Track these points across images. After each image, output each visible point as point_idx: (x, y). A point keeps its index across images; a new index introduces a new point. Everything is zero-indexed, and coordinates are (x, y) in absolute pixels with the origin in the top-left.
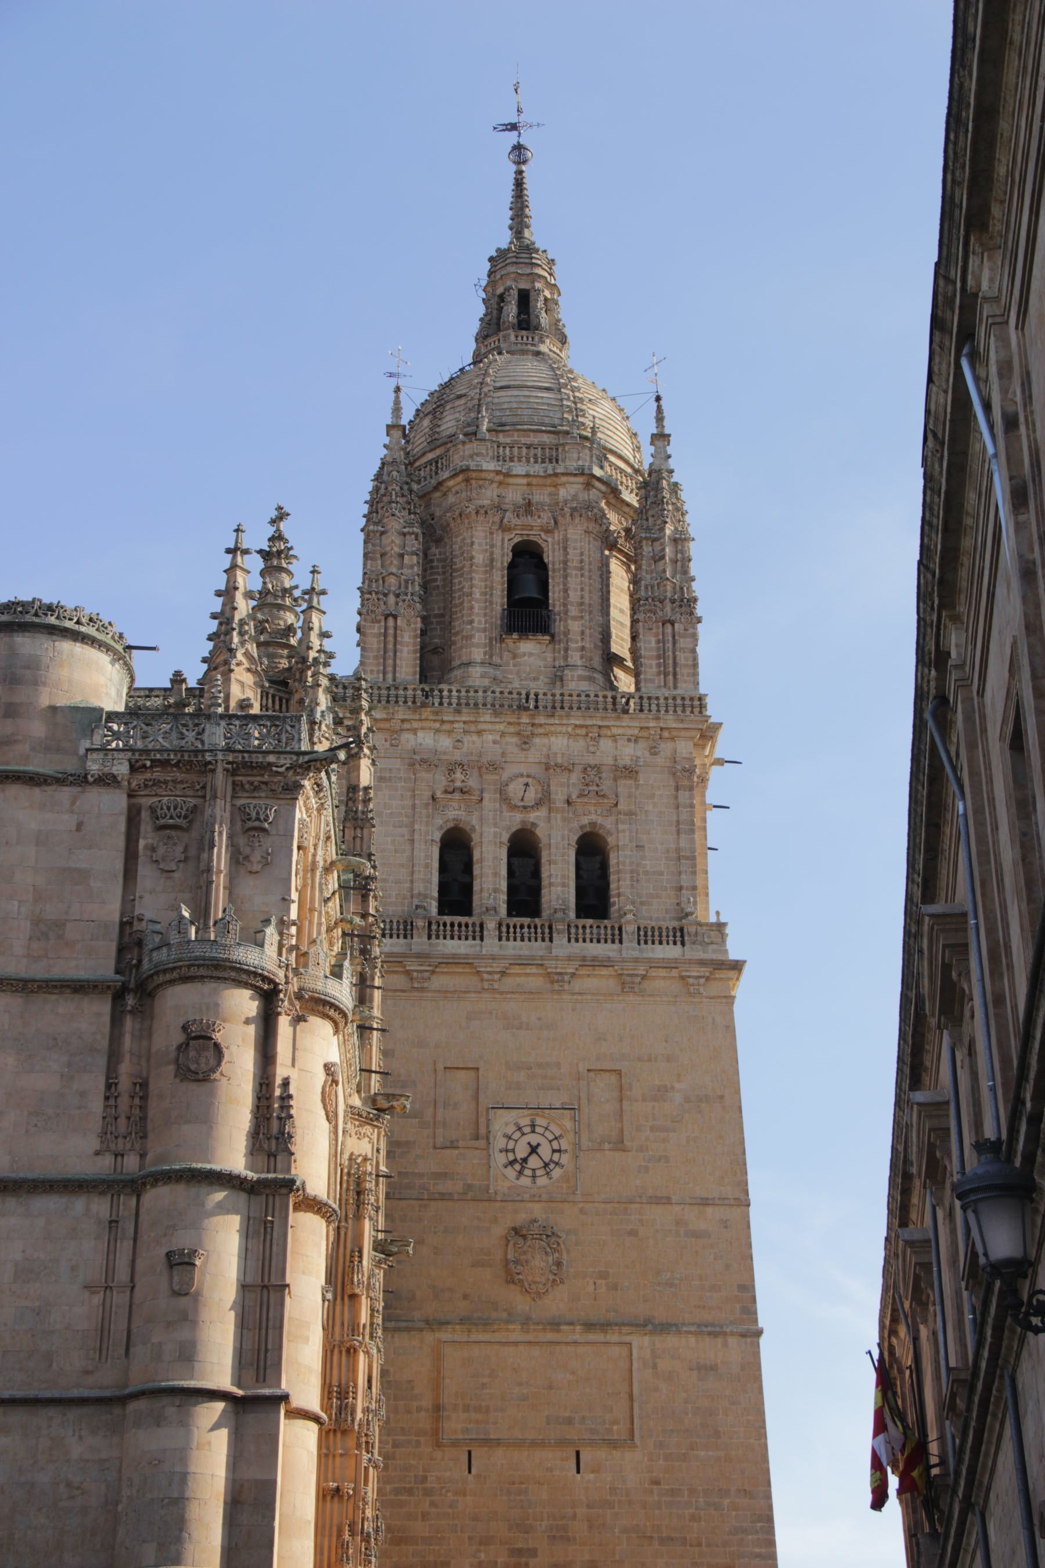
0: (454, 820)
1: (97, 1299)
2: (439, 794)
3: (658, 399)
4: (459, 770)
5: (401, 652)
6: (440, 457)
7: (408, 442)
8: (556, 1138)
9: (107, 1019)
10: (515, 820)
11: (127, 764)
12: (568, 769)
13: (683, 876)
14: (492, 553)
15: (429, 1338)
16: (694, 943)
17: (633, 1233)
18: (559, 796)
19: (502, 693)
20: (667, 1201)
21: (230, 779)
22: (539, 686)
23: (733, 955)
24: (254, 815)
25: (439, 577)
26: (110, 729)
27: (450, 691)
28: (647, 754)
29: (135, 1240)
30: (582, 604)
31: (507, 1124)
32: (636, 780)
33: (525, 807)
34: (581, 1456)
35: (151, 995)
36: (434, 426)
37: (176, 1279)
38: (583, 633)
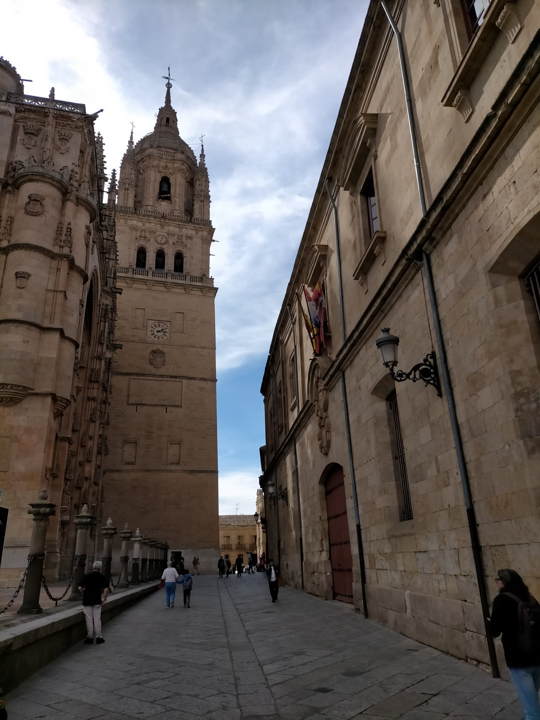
0: (141, 245)
2: (138, 237)
3: (202, 146)
4: (144, 231)
5: (129, 199)
10: (159, 246)
15: (127, 377)
16: (205, 282)
18: (171, 242)
21: (55, 121)
22: (167, 213)
24: (63, 134)
25: (141, 183)
27: (142, 211)
29: (4, 271)
30: (180, 194)
33: (161, 244)
35: (18, 188)
38: (179, 202)
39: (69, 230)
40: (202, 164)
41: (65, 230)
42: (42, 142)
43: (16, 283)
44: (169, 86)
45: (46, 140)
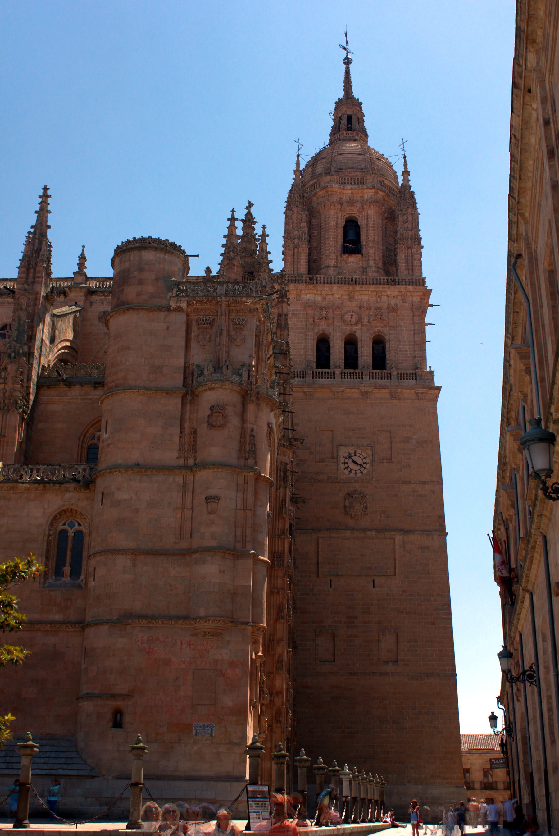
1: (179, 515)
3: (405, 157)
4: (324, 310)
5: (300, 262)
6: (316, 183)
7: (302, 177)
8: (365, 458)
9: (180, 405)
10: (348, 330)
11: (186, 302)
12: (370, 309)
13: (416, 352)
14: (337, 221)
16: (421, 379)
17: (396, 495)
18: (365, 320)
19: (341, 278)
20: (410, 482)
22: (357, 276)
23: (436, 384)
24: (237, 323)
25: (316, 232)
26: (180, 289)
27: (320, 278)
28: (401, 302)
29: (193, 493)
30: (374, 241)
31: (344, 452)
32: (397, 313)
33: (351, 325)
34: (375, 582)
36: (313, 170)
37: (209, 508)
38: (374, 253)
39: (253, 436)
40: (406, 187)
41: (248, 439)
42: (216, 336)
43: (207, 508)
44: (348, 62)
45: (221, 334)
